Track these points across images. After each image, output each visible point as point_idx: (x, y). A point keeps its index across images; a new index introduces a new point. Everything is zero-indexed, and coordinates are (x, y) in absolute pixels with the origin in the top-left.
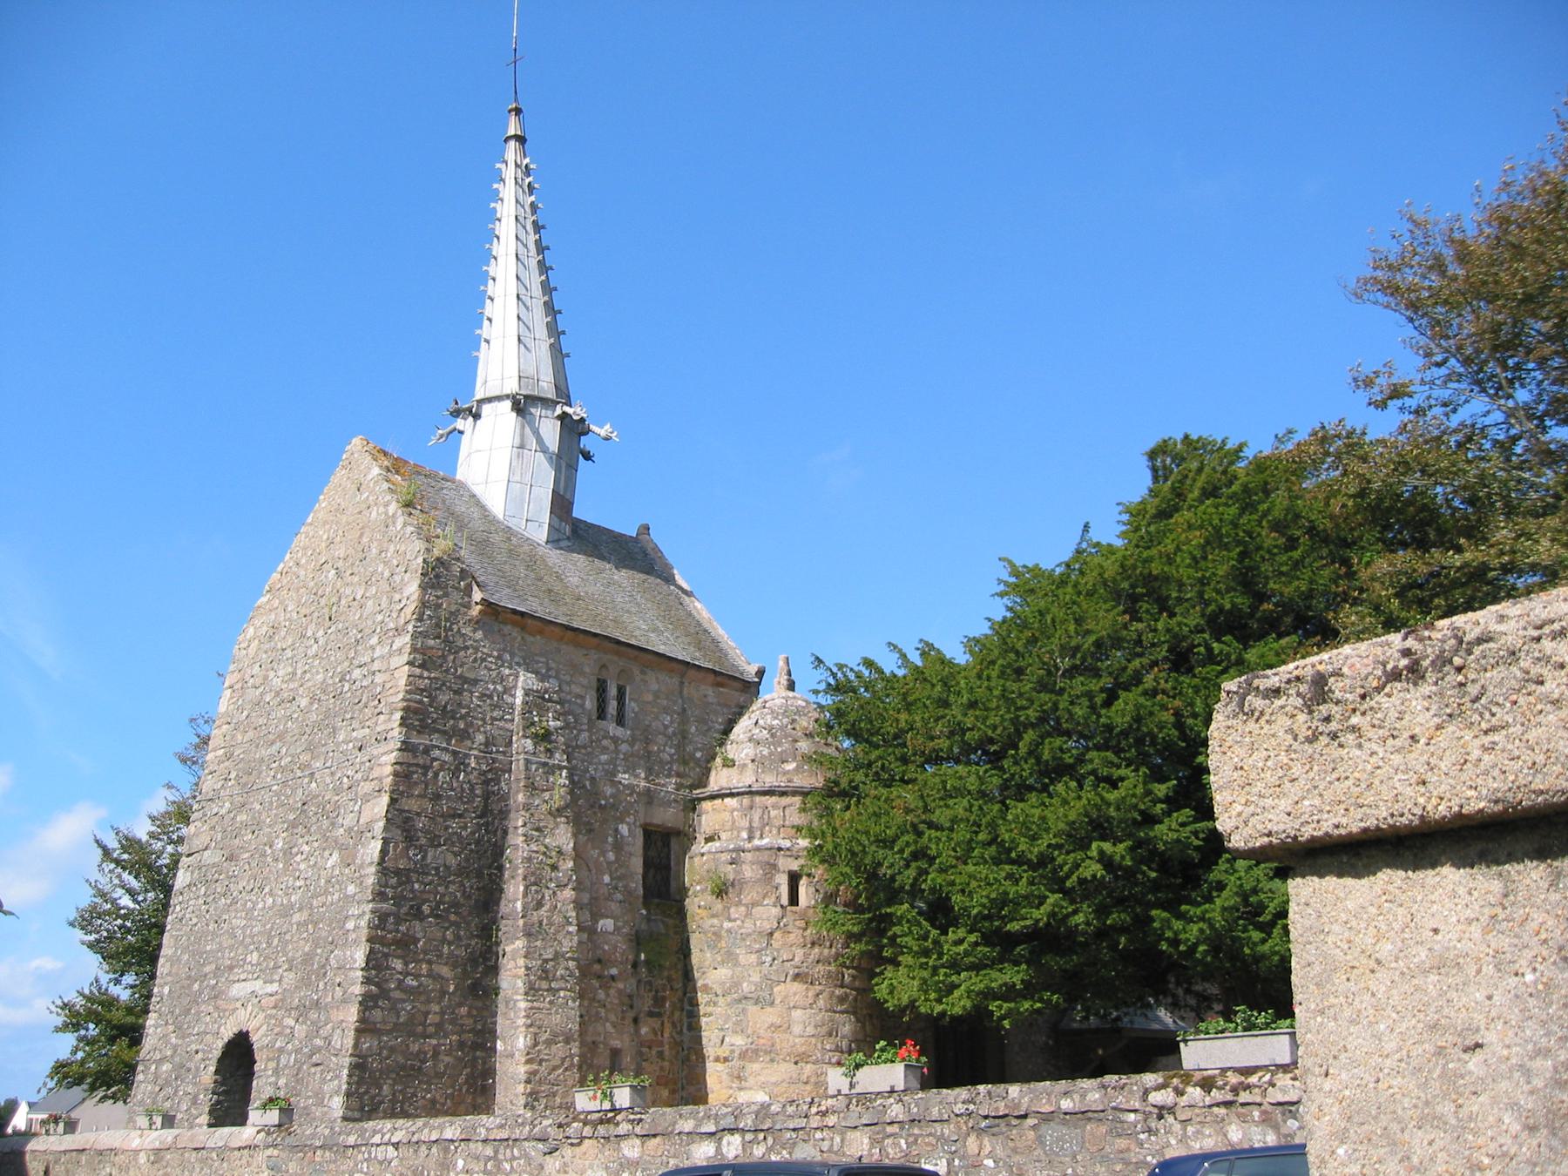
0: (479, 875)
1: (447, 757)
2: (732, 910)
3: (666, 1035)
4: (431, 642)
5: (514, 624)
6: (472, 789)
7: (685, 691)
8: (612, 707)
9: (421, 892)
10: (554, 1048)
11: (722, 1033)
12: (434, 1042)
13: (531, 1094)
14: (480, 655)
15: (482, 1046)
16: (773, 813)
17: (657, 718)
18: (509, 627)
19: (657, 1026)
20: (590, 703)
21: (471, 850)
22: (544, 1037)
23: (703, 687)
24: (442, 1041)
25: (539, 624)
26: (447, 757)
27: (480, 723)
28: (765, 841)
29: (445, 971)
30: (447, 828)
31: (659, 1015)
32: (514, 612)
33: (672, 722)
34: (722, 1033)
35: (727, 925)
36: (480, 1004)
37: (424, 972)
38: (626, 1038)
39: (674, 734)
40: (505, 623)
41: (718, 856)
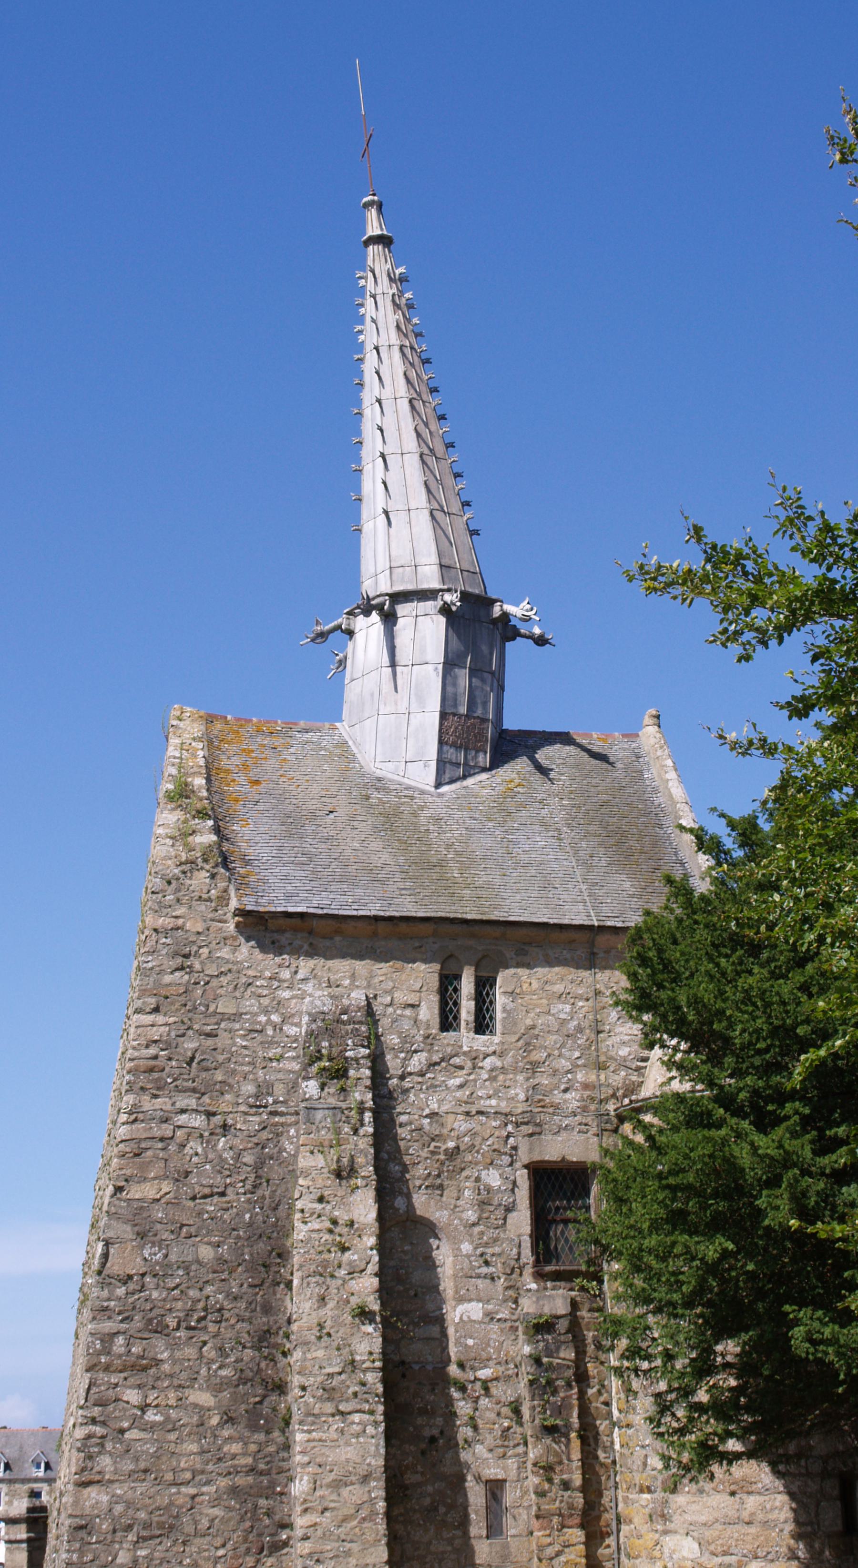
0: (251, 1268)
1: (198, 1121)
4: (168, 979)
5: (295, 930)
6: (238, 1157)
8: (467, 1008)
9: (164, 1300)
10: (345, 1492)
11: (644, 1452)
12: (192, 1491)
13: (310, 1555)
14: (244, 980)
15: (269, 1492)
18: (288, 935)
20: (429, 1011)
21: (238, 1237)
22: (332, 1476)
24: (205, 1489)
25: (330, 922)
26: (198, 1121)
27: (246, 1069)
29: (203, 1398)
30: (200, 1214)
32: (287, 915)
34: (644, 1452)
36: (261, 1437)
37: (172, 1402)
38: (512, 1463)
39: (580, 1029)
40: (281, 931)
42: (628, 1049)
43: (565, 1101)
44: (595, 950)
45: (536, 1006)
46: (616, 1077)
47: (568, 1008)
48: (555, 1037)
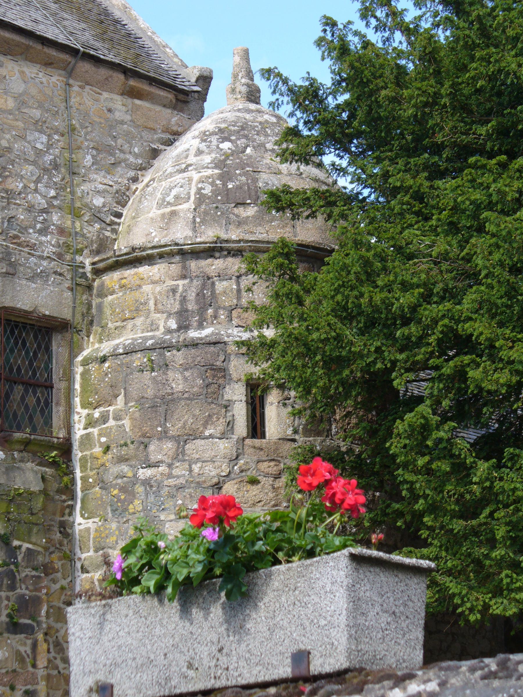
2: (152, 448)
3: (42, 663)
7: (74, 101)
16: (220, 286)
17: (23, 138)
19: (26, 649)
23: (105, 95)
28: (207, 331)
31: (28, 630)
33: (49, 146)
35: (144, 473)
41: (127, 359)
42: (102, 200)
43: (41, 243)
44: (71, 81)
45: (13, 127)
46: (90, 228)
47: (44, 139)
48: (31, 168)
